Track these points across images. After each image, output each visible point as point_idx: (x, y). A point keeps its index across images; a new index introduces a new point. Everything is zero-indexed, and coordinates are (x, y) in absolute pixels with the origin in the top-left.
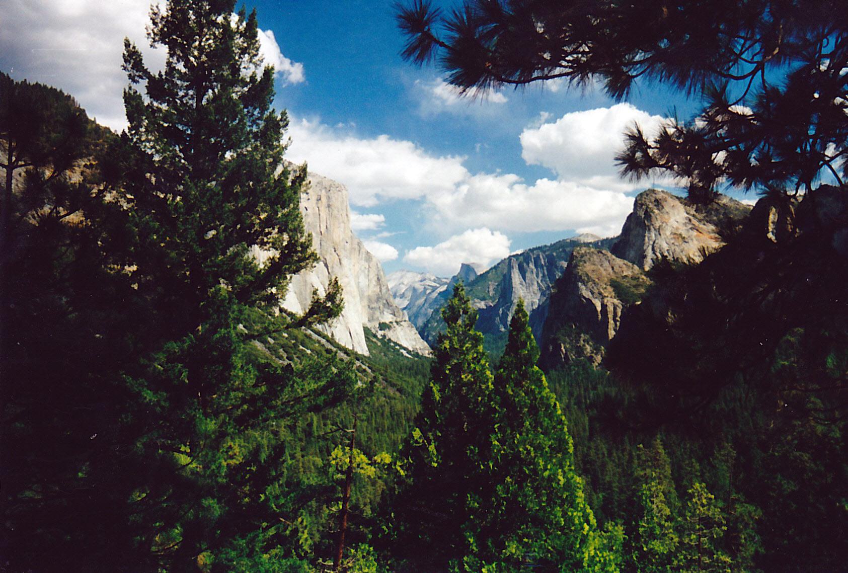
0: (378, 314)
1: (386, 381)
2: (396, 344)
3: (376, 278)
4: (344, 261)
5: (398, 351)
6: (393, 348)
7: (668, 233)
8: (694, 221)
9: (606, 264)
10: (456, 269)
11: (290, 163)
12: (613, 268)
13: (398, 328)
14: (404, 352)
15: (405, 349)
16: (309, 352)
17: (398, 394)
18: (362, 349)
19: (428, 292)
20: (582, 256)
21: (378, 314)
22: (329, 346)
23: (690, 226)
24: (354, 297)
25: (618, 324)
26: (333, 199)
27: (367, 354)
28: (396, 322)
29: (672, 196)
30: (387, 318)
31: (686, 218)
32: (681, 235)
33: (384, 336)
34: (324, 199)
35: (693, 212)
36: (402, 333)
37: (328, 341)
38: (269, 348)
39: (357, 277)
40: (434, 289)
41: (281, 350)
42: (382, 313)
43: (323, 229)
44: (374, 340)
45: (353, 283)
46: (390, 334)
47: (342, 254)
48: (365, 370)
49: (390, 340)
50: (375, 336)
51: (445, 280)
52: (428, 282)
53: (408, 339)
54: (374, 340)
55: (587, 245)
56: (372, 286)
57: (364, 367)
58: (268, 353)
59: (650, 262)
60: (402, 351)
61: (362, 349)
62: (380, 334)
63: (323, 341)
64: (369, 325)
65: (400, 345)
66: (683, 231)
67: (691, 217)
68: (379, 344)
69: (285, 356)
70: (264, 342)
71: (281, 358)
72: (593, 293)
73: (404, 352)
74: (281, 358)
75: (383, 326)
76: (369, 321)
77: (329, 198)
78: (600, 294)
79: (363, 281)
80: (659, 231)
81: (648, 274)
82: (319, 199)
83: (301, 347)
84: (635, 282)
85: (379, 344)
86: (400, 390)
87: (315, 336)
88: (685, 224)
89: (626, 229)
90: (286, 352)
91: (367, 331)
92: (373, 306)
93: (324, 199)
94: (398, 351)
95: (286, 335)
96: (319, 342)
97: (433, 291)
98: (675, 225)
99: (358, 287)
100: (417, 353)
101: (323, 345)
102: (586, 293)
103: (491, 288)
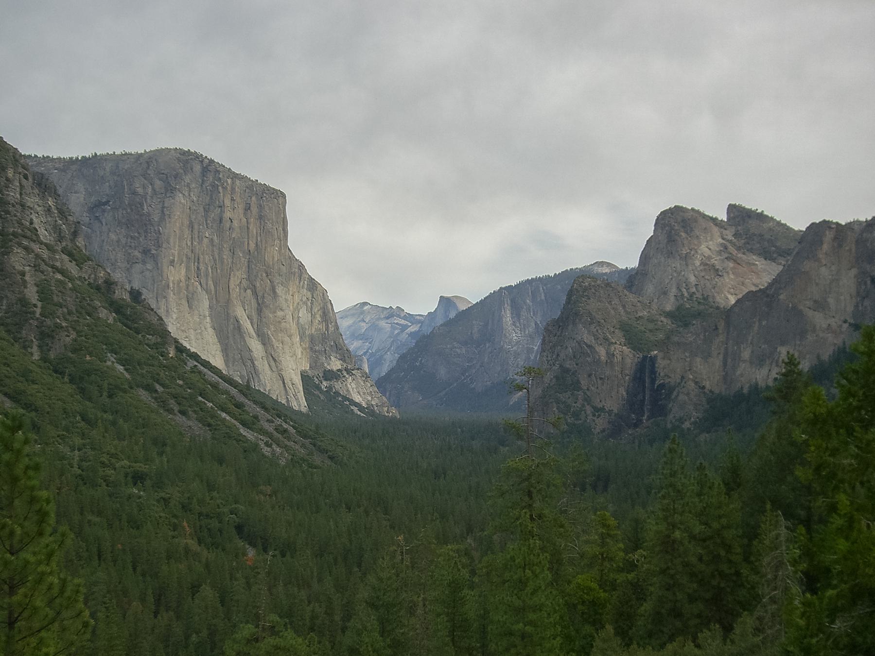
1: (315, 446)
2: (346, 398)
4: (280, 290)
5: (348, 407)
7: (698, 263)
8: (731, 249)
9: (616, 301)
10: (432, 307)
11: (212, 161)
12: (624, 307)
14: (355, 409)
16: (210, 405)
17: (328, 462)
18: (299, 403)
19: (396, 332)
20: (586, 289)
22: (242, 399)
23: (727, 255)
24: (290, 336)
25: (627, 378)
26: (266, 208)
27: (304, 409)
28: (346, 369)
29: (704, 216)
30: (335, 364)
31: (721, 244)
32: (713, 266)
33: (330, 388)
34: (255, 210)
35: (730, 237)
36: (354, 386)
37: (240, 391)
38: (156, 399)
39: (297, 309)
40: (404, 328)
41: (172, 401)
42: (328, 358)
43: (252, 246)
46: (338, 386)
47: (277, 280)
48: (285, 431)
49: (337, 393)
50: (318, 387)
51: (418, 317)
52: (397, 320)
53: (359, 392)
55: (594, 278)
57: (285, 426)
58: (155, 405)
59: (672, 299)
63: (234, 391)
64: (310, 373)
65: (348, 400)
67: (728, 244)
69: (176, 408)
70: (149, 388)
71: (170, 411)
72: (597, 339)
73: (355, 409)
74: (170, 411)
75: (330, 375)
77: (260, 207)
78: (606, 339)
79: (304, 315)
80: (686, 258)
81: (669, 315)
82: (248, 208)
83: (200, 398)
84: (651, 326)
86: (331, 458)
87: (224, 385)
88: (719, 253)
89: (645, 258)
90: (179, 404)
91: (306, 378)
93: (255, 210)
94: (348, 407)
95: (181, 382)
96: (227, 393)
97: (402, 331)
98: (707, 253)
99: (298, 323)
100: (373, 411)
101: (233, 397)
102: (588, 338)
103: (476, 330)
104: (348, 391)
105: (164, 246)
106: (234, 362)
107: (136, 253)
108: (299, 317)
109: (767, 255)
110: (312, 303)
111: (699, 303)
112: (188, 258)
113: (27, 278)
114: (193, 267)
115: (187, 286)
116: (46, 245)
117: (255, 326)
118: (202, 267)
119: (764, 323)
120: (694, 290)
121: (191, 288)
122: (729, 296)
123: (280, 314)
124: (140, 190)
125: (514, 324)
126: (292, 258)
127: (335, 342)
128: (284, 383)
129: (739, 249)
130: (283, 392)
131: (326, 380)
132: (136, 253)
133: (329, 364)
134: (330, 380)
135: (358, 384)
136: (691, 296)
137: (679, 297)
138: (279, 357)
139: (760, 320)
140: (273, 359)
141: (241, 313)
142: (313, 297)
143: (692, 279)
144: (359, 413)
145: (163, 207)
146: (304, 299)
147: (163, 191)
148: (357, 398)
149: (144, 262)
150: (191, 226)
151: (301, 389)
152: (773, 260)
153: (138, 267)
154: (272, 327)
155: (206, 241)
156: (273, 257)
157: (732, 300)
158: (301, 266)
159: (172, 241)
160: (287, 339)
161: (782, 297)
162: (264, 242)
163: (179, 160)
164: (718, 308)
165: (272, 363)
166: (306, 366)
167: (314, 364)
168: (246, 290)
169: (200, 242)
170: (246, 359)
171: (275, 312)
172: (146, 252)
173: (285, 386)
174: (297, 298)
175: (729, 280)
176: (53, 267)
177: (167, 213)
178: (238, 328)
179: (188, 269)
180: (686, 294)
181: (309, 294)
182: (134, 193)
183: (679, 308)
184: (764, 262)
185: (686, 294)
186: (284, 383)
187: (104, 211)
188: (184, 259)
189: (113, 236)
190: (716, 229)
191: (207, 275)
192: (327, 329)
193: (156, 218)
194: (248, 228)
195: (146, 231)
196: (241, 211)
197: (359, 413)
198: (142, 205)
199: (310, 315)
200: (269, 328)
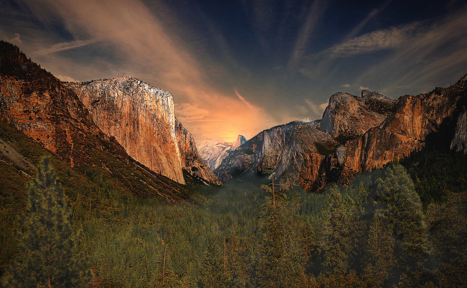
2: (201, 178)
3: (189, 143)
6: (199, 180)
13: (202, 170)
14: (205, 182)
15: (205, 181)
18: (182, 181)
27: (184, 184)
28: (201, 166)
30: (196, 165)
33: (194, 174)
46: (197, 173)
49: (197, 176)
50: (189, 174)
61: (182, 181)
62: (192, 173)
64: (186, 168)
66: (357, 116)
73: (205, 182)
75: (194, 169)
76: (186, 166)
81: (336, 139)
99: (180, 148)
104: (202, 176)
105: (124, 118)
107: (112, 121)
109: (380, 112)
111: (350, 134)
112: (134, 123)
113: (67, 133)
114: (136, 126)
116: (74, 119)
118: (140, 127)
119: (379, 141)
120: (347, 128)
121: (135, 135)
122: (363, 130)
124: (112, 95)
129: (367, 109)
130: (175, 176)
131: (192, 171)
132: (112, 121)
136: (346, 131)
137: (341, 131)
139: (377, 140)
140: (171, 163)
141: (155, 145)
143: (346, 123)
145: (122, 102)
147: (122, 95)
148: (206, 178)
149: (115, 125)
150: (133, 109)
151: (182, 175)
152: (383, 113)
153: (113, 127)
154: (170, 150)
155: (140, 115)
157: (364, 132)
158: (180, 125)
159: (126, 116)
161: (386, 129)
163: (128, 82)
164: (358, 135)
165: (170, 165)
167: (187, 165)
169: (138, 115)
170: (158, 163)
172: (116, 121)
175: (362, 123)
176: (77, 128)
177: (124, 104)
178: (155, 151)
179: (134, 127)
180: (343, 130)
182: (110, 96)
183: (340, 136)
184: (379, 115)
185: (343, 130)
187: (97, 104)
188: (132, 123)
189: (102, 115)
190: (356, 102)
191: (142, 129)
193: (120, 106)
195: (115, 112)
196: (155, 103)
198: (113, 101)
200: (168, 150)
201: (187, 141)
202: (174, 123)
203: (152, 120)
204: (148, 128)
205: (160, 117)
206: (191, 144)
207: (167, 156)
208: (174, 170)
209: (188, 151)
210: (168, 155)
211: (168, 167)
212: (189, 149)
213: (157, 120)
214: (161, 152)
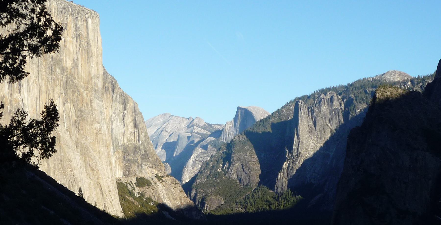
0: (134, 168)
3: (132, 124)
13: (160, 186)
18: (115, 210)
21: (134, 168)
28: (157, 176)
33: (142, 194)
36: (164, 192)
39: (111, 121)
44: (130, 198)
45: (105, 129)
46: (149, 192)
49: (149, 199)
54: (130, 198)
56: (127, 133)
60: (164, 212)
62: (137, 191)
64: (124, 181)
68: (136, 203)
75: (142, 182)
79: (117, 126)
85: (136, 203)
92: (130, 157)
99: (112, 135)
106: (54, 171)
108: (112, 129)
110: (124, 115)
115: (11, 101)
117: (74, 138)
123: (97, 126)
125: (311, 132)
126: (105, 74)
127: (145, 151)
128: (101, 191)
133: (141, 172)
134: (142, 187)
135: (168, 191)
138: (96, 165)
140: (92, 169)
142: (124, 110)
144: (170, 217)
146: (117, 112)
151: (117, 195)
156: (89, 73)
160: (102, 149)
162: (80, 60)
165: (90, 172)
166: (119, 174)
168: (64, 104)
171: (91, 125)
173: (102, 193)
174: (111, 113)
181: (122, 106)
186: (101, 191)
192: (139, 139)
194: (65, 46)
197: (170, 217)
199: (122, 126)
200: (86, 139)
201: (129, 120)
202: (101, 79)
203: (52, 70)
204: (44, 88)
205: (69, 64)
206: (136, 125)
207: (84, 151)
208: (99, 185)
209: (129, 141)
210: (87, 149)
211: (85, 176)
212: (132, 137)
213: (63, 70)
214: (71, 144)
